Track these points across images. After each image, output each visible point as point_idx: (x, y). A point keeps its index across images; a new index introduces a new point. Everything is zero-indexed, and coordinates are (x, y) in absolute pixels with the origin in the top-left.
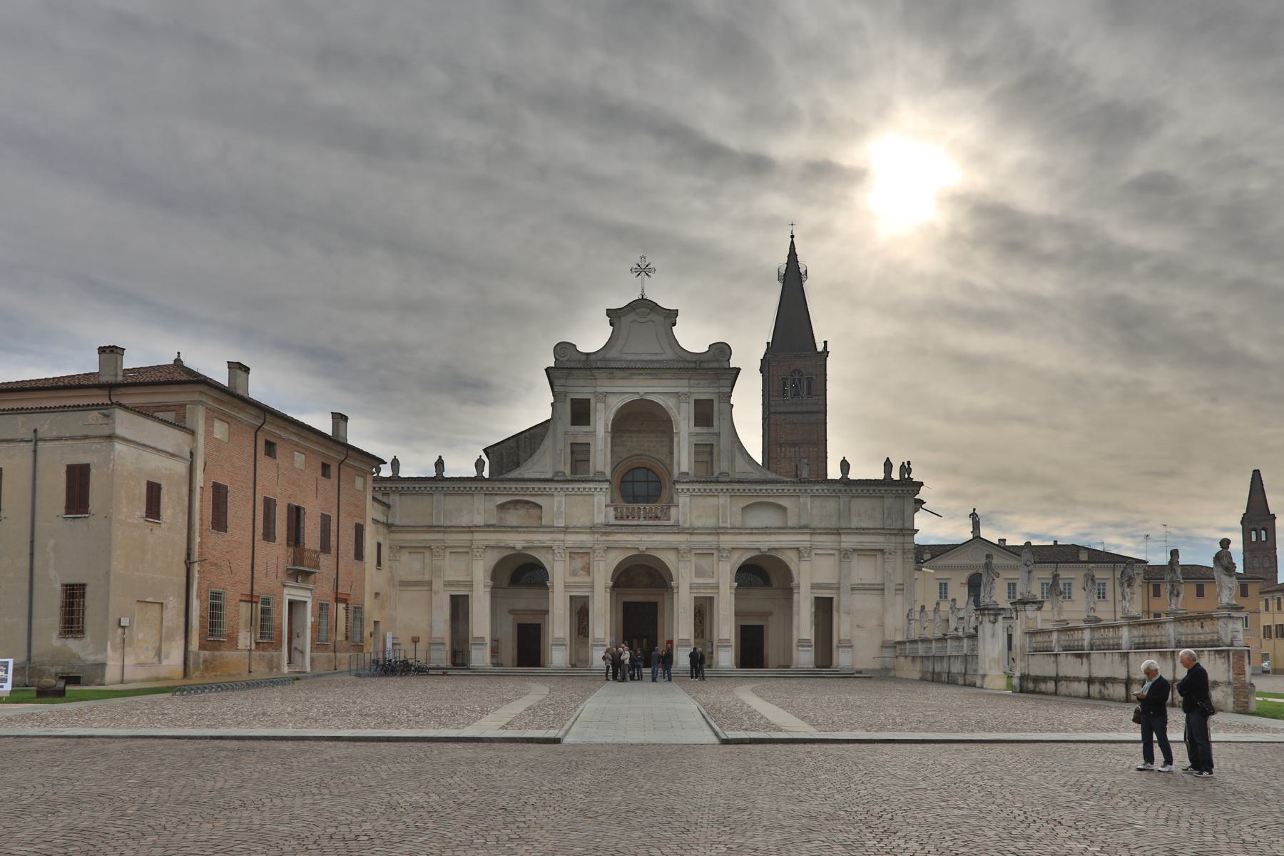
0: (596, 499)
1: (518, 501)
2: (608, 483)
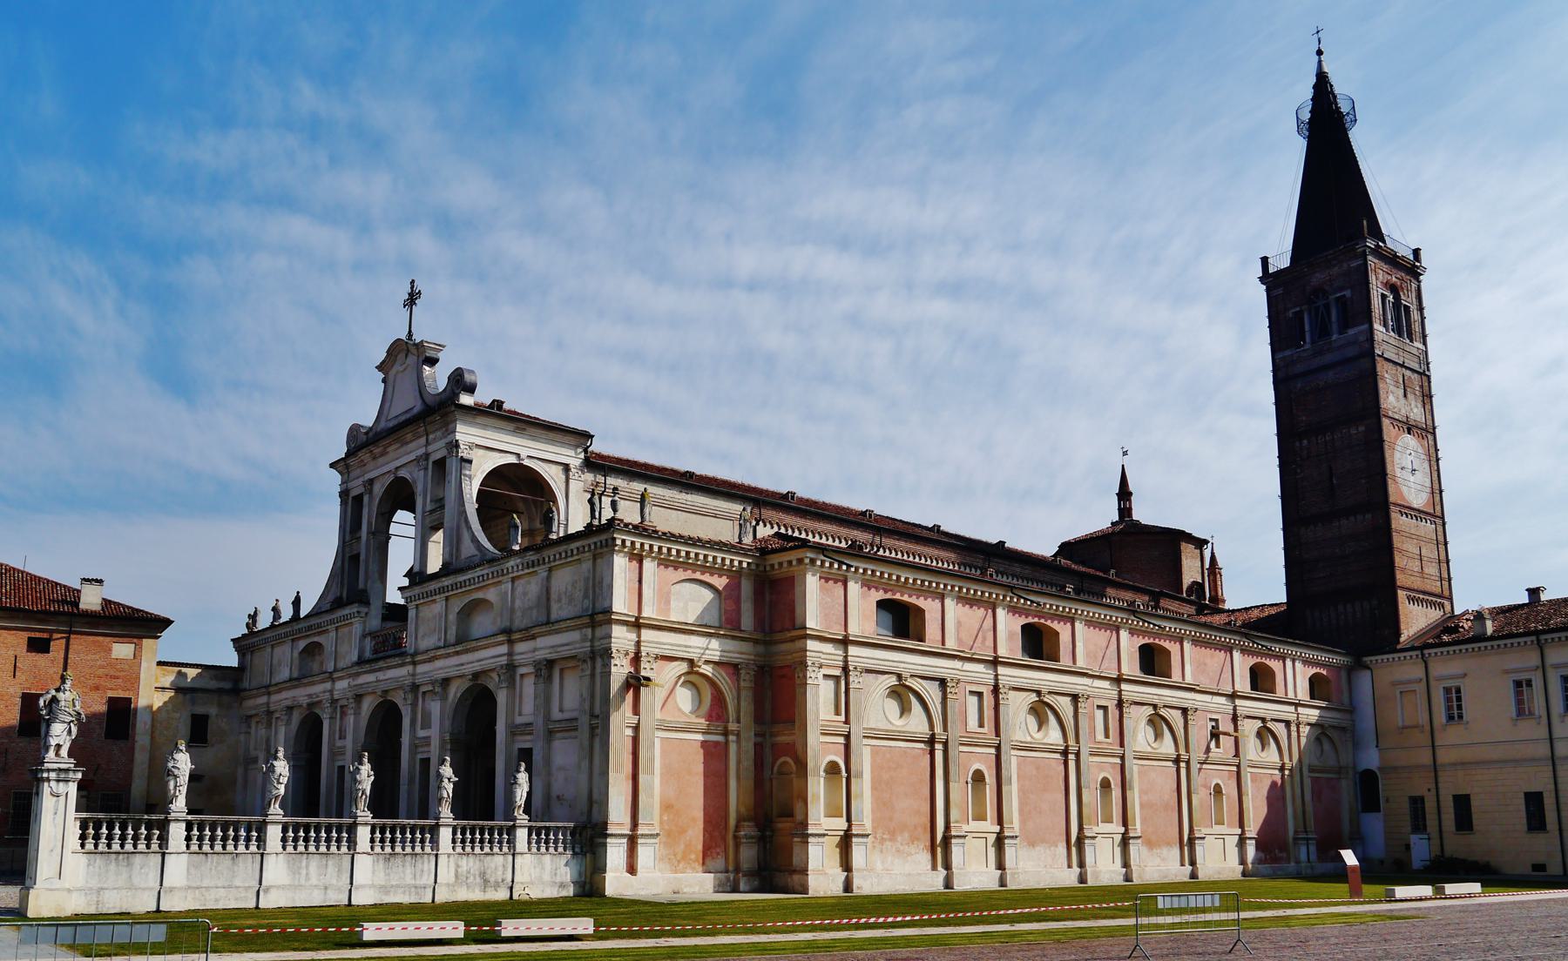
0: (354, 627)
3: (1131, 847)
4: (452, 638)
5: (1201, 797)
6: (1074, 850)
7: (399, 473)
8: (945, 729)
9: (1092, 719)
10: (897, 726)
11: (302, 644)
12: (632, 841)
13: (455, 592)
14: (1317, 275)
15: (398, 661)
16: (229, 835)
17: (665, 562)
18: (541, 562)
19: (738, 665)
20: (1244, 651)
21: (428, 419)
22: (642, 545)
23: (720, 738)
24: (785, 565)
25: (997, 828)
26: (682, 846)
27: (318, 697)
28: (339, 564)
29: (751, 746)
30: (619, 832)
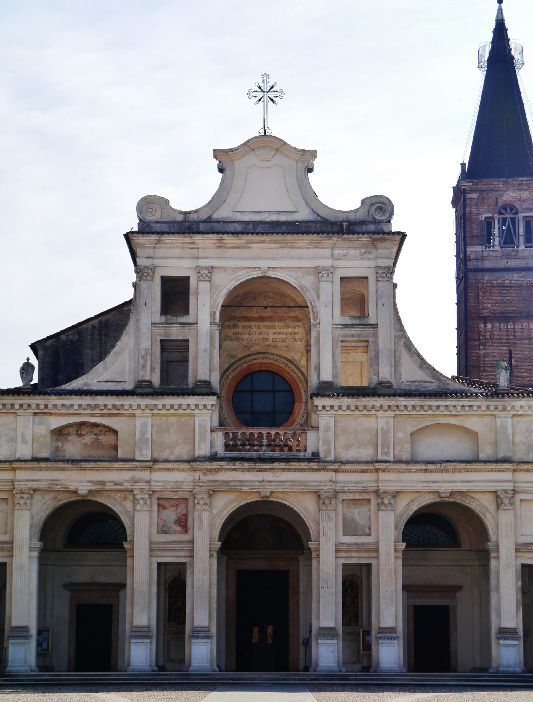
1: (82, 424)
2: (215, 398)
14: (509, 192)
15: (313, 465)
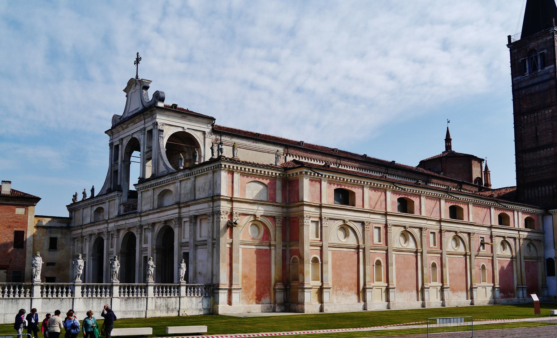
3: (445, 292)
4: (156, 206)
5: (476, 270)
6: (420, 293)
7: (133, 135)
8: (364, 243)
9: (428, 238)
10: (343, 242)
11: (95, 208)
12: (230, 291)
13: (157, 186)
14: (532, 43)
15: (134, 215)
16: (59, 291)
17: (243, 174)
18: (191, 174)
19: (275, 217)
20: (496, 208)
21: (145, 113)
22: (233, 167)
23: (267, 248)
24: (295, 174)
25: (386, 285)
26: (252, 293)
27: (102, 230)
28: (110, 174)
29: (281, 250)
30: (224, 288)
